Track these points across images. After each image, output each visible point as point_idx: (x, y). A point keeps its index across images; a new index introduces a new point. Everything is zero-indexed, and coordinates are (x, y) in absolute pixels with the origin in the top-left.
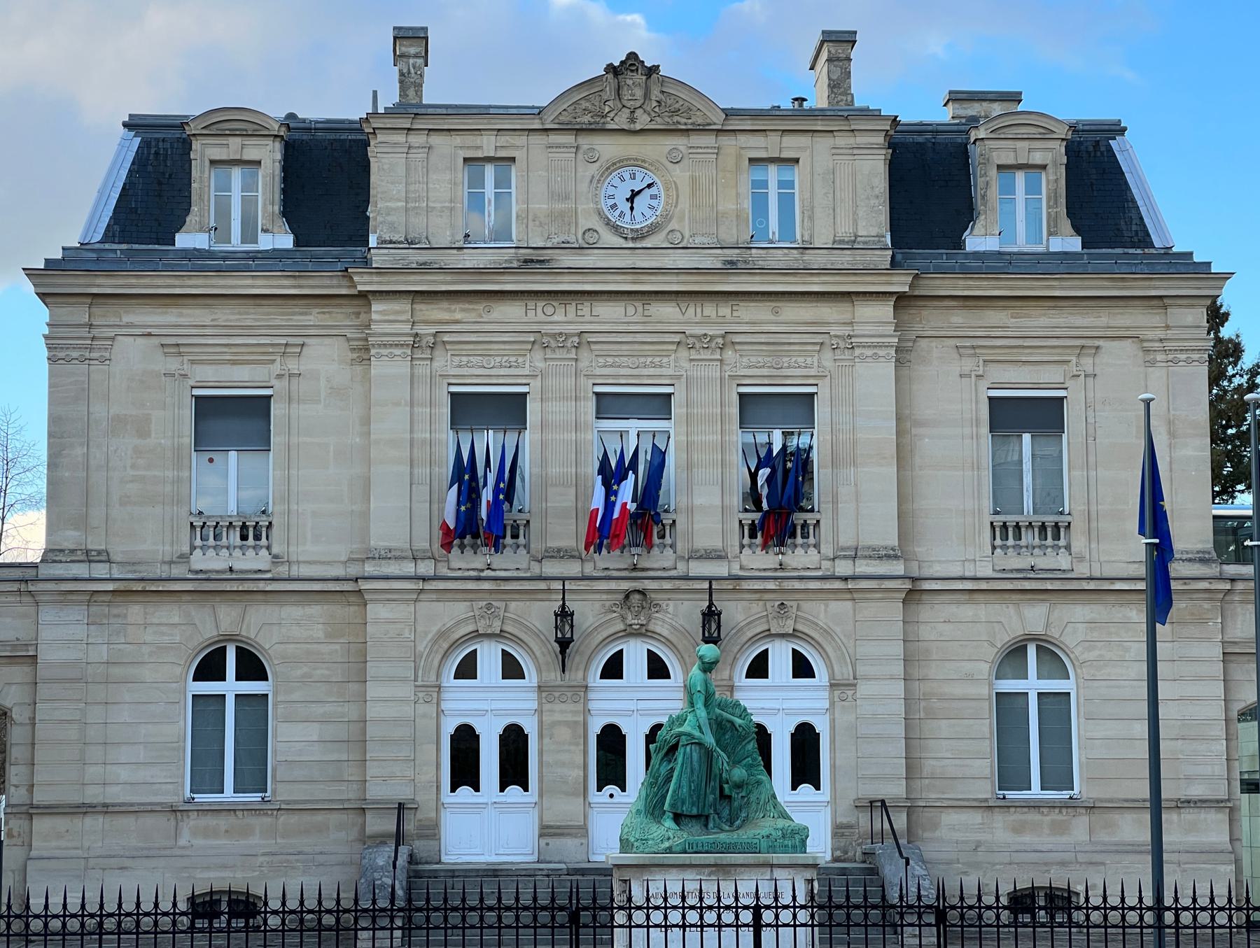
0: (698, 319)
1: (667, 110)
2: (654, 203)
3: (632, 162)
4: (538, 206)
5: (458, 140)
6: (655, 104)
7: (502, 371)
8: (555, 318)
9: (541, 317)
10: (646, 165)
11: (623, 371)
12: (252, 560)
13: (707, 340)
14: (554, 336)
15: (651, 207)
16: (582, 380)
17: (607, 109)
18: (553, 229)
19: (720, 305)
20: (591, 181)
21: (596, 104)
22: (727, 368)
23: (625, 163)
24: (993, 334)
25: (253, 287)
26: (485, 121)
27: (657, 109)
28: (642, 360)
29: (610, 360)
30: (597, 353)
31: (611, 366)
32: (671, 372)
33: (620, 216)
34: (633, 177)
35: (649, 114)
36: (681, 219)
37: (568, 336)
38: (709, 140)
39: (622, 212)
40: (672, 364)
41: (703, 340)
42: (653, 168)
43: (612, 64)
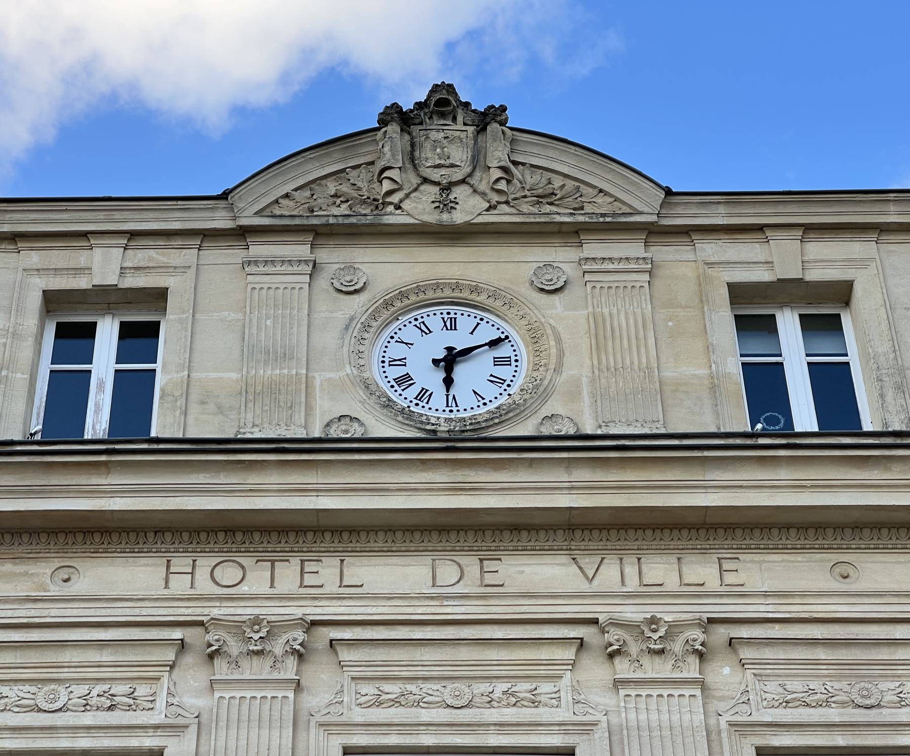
0: (632, 584)
1: (528, 193)
2: (504, 372)
3: (448, 293)
4: (213, 375)
5: (33, 257)
6: (497, 174)
8: (244, 588)
9: (204, 586)
10: (482, 298)
11: (425, 715)
13: (661, 632)
14: (237, 628)
16: (313, 737)
17: (387, 186)
18: (250, 416)
19: (688, 558)
20: (347, 328)
21: (359, 184)
22: (722, 706)
23: (430, 294)
26: (101, 216)
27: (502, 185)
28: (483, 687)
29: (393, 689)
30: (356, 672)
31: (396, 702)
32: (563, 714)
33: (419, 397)
34: (451, 325)
35: (483, 194)
36: (573, 396)
37: (274, 629)
38: (633, 248)
39: (424, 391)
40: (567, 697)
41: (650, 634)
42: (498, 303)
43: (395, 106)
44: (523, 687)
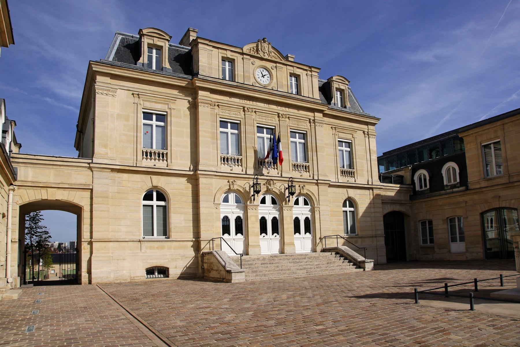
7: (234, 116)
12: (161, 164)
15: (268, 80)
24: (338, 125)
25: (163, 80)
44: (272, 119)
